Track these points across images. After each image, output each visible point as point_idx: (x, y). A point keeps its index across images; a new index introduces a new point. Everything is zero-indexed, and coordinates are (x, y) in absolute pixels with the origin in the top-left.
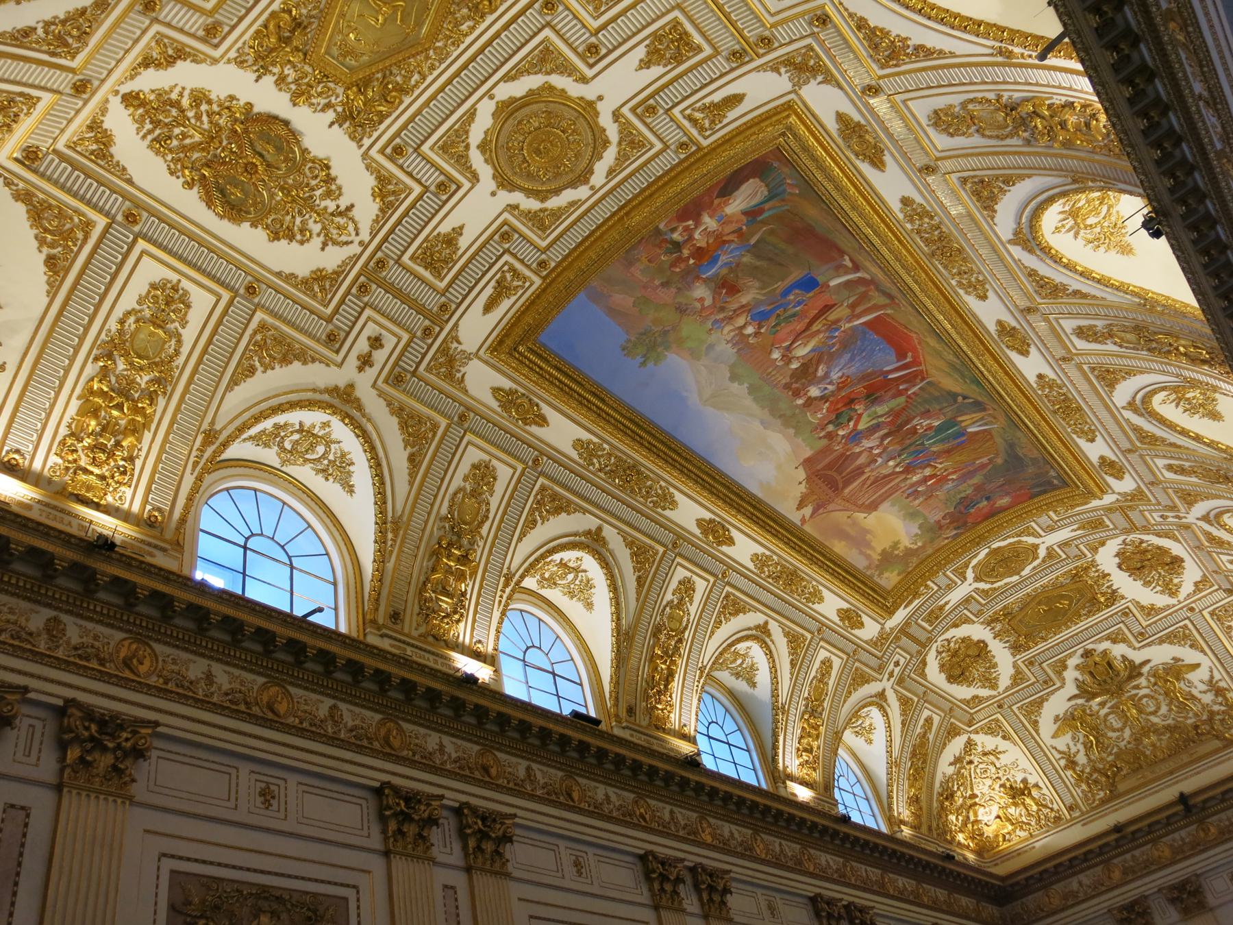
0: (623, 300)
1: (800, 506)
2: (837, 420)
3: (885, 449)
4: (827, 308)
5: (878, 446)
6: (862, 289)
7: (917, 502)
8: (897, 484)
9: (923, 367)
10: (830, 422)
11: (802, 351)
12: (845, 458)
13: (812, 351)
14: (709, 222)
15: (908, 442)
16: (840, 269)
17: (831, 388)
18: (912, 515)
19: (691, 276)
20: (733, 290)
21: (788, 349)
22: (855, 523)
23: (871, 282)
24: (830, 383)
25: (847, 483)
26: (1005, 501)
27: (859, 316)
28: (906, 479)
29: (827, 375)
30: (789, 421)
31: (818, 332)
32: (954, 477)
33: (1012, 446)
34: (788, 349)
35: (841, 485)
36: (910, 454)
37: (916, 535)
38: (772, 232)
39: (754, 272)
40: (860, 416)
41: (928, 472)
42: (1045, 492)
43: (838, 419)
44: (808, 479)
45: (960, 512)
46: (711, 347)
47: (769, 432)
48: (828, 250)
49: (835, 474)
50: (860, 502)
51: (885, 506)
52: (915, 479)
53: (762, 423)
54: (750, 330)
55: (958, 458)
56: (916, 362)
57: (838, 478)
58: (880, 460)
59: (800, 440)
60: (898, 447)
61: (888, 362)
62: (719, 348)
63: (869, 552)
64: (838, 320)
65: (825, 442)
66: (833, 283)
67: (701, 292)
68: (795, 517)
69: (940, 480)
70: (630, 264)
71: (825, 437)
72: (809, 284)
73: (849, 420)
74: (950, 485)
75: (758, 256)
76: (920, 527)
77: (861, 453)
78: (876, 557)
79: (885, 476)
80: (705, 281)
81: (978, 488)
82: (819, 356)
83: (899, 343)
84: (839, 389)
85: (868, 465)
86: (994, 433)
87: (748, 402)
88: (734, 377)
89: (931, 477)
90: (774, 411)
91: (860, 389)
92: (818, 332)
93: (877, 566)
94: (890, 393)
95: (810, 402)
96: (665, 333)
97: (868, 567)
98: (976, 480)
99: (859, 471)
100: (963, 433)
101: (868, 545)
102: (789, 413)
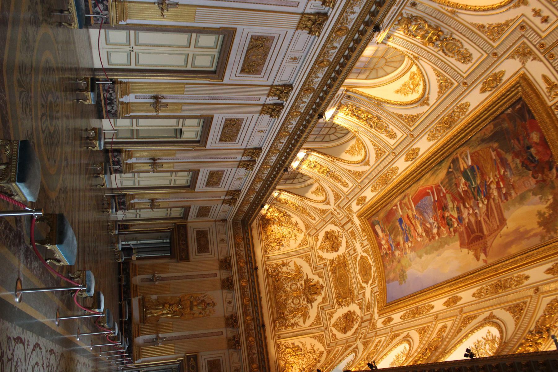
0: (392, 276)
1: (478, 259)
2: (449, 225)
3: (471, 207)
4: (408, 217)
5: (469, 210)
6: (403, 205)
7: (513, 194)
8: (495, 204)
9: (434, 186)
10: (449, 229)
11: (420, 230)
12: (469, 228)
13: (421, 226)
14: (383, 242)
15: (471, 195)
16: (397, 210)
17: (435, 224)
18: (522, 199)
19: (393, 253)
20: (398, 244)
21: (418, 234)
22: (507, 235)
23: (401, 201)
24: (434, 223)
25: (481, 231)
26: (535, 137)
27: (412, 207)
28: (494, 199)
29: (430, 224)
30: (442, 245)
31: (415, 222)
32: (502, 171)
33: (483, 140)
34: (418, 234)
35: (481, 234)
36: (479, 195)
37: (541, 198)
38: (387, 227)
39: (395, 236)
40: (451, 215)
41: (493, 186)
42: (529, 111)
43: (449, 225)
44: (469, 248)
45: (534, 167)
46: (410, 259)
47: (442, 255)
48: (391, 214)
49: (474, 235)
50: (496, 227)
51: (506, 214)
52: (495, 193)
53: (438, 256)
54: (410, 244)
55: (489, 169)
56: (431, 188)
57: (476, 234)
58: (477, 211)
59: (451, 244)
60: (473, 200)
61: (431, 199)
62: (411, 257)
63: (532, 233)
64: (412, 214)
65: (457, 234)
66: (401, 213)
67: (397, 253)
68: (481, 264)
69: (503, 180)
70: (386, 267)
71: (455, 233)
72: (401, 221)
73: (451, 220)
74: (508, 173)
75: (392, 233)
76: (535, 194)
77: (469, 219)
78: (540, 230)
79: (487, 210)
80: (395, 250)
81: (517, 155)
82: (423, 224)
83: (423, 194)
84: (437, 221)
85: (476, 217)
86: (472, 152)
87: (429, 256)
88: (420, 257)
89: (498, 183)
90: (437, 250)
91: (439, 212)
92: (415, 222)
93: (548, 231)
94: (444, 200)
95: (438, 234)
96: (402, 270)
97: (543, 237)
98: (509, 158)
99: (478, 223)
100: (472, 168)
101: (527, 232)
102: (439, 244)
